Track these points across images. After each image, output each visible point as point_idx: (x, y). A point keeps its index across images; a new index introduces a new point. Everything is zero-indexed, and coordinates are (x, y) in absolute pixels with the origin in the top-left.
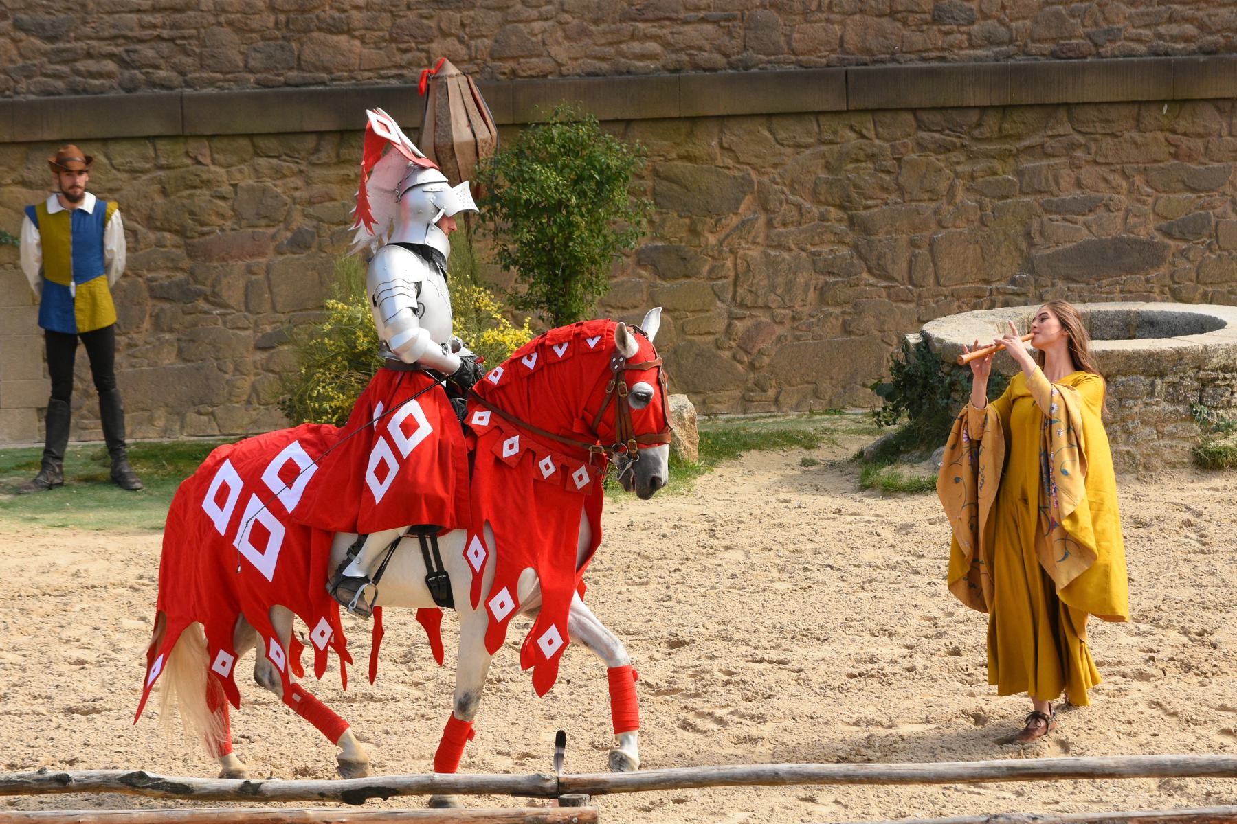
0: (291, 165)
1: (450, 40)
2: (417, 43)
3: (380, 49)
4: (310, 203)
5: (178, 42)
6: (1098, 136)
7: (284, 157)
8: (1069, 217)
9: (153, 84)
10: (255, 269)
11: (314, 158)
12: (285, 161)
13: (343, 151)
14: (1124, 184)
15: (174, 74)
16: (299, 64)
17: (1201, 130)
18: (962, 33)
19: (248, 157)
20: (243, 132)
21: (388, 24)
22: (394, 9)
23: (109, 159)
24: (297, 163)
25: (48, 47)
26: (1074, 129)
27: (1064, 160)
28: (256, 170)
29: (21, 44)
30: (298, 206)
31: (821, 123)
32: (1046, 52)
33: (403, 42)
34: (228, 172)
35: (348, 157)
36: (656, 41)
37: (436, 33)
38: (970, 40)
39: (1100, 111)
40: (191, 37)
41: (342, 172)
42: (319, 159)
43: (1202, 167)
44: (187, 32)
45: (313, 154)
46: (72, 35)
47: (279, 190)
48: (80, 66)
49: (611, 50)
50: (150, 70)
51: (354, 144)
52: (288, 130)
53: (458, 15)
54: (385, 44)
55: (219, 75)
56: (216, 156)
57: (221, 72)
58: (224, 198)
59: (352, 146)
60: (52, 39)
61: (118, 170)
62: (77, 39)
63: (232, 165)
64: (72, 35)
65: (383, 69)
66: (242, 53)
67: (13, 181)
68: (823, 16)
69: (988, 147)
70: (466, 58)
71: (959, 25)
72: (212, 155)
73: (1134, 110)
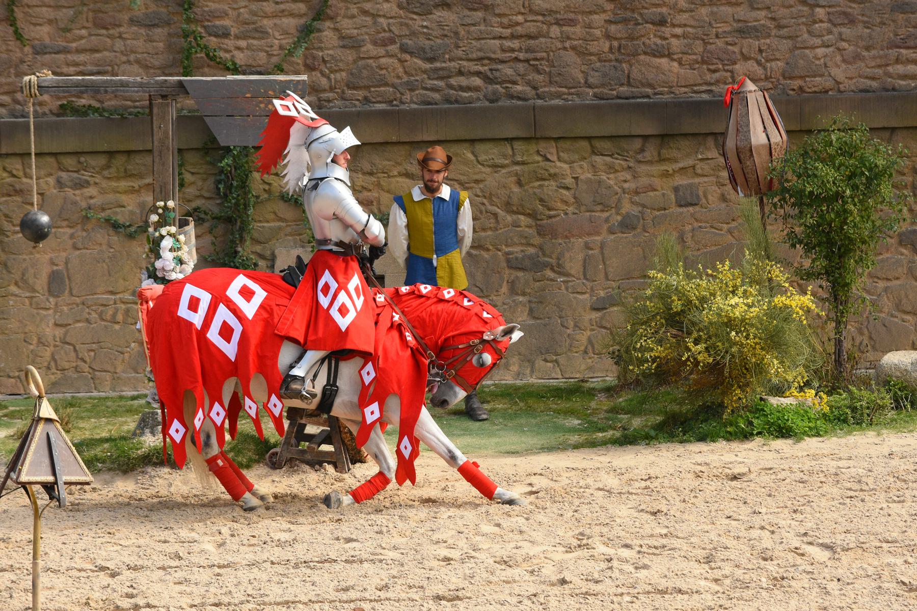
0: (621, 162)
1: (750, 62)
2: (724, 65)
3: (694, 69)
4: (637, 193)
5: (532, 62)
7: (616, 156)
9: (512, 97)
10: (591, 245)
11: (640, 157)
12: (617, 159)
13: (664, 151)
15: (528, 89)
16: (629, 82)
19: (586, 155)
23: (476, 156)
24: (626, 160)
25: (428, 66)
28: (593, 166)
40: (542, 59)
44: (539, 55)
45: (639, 153)
46: (447, 56)
47: (612, 182)
48: (453, 81)
50: (510, 85)
55: (564, 90)
56: (562, 154)
57: (566, 87)
58: (568, 188)
59: (671, 147)
60: (432, 60)
61: (483, 165)
62: (451, 60)
63: (573, 162)
64: (447, 56)
66: (583, 72)
67: (399, 173)
70: (763, 77)
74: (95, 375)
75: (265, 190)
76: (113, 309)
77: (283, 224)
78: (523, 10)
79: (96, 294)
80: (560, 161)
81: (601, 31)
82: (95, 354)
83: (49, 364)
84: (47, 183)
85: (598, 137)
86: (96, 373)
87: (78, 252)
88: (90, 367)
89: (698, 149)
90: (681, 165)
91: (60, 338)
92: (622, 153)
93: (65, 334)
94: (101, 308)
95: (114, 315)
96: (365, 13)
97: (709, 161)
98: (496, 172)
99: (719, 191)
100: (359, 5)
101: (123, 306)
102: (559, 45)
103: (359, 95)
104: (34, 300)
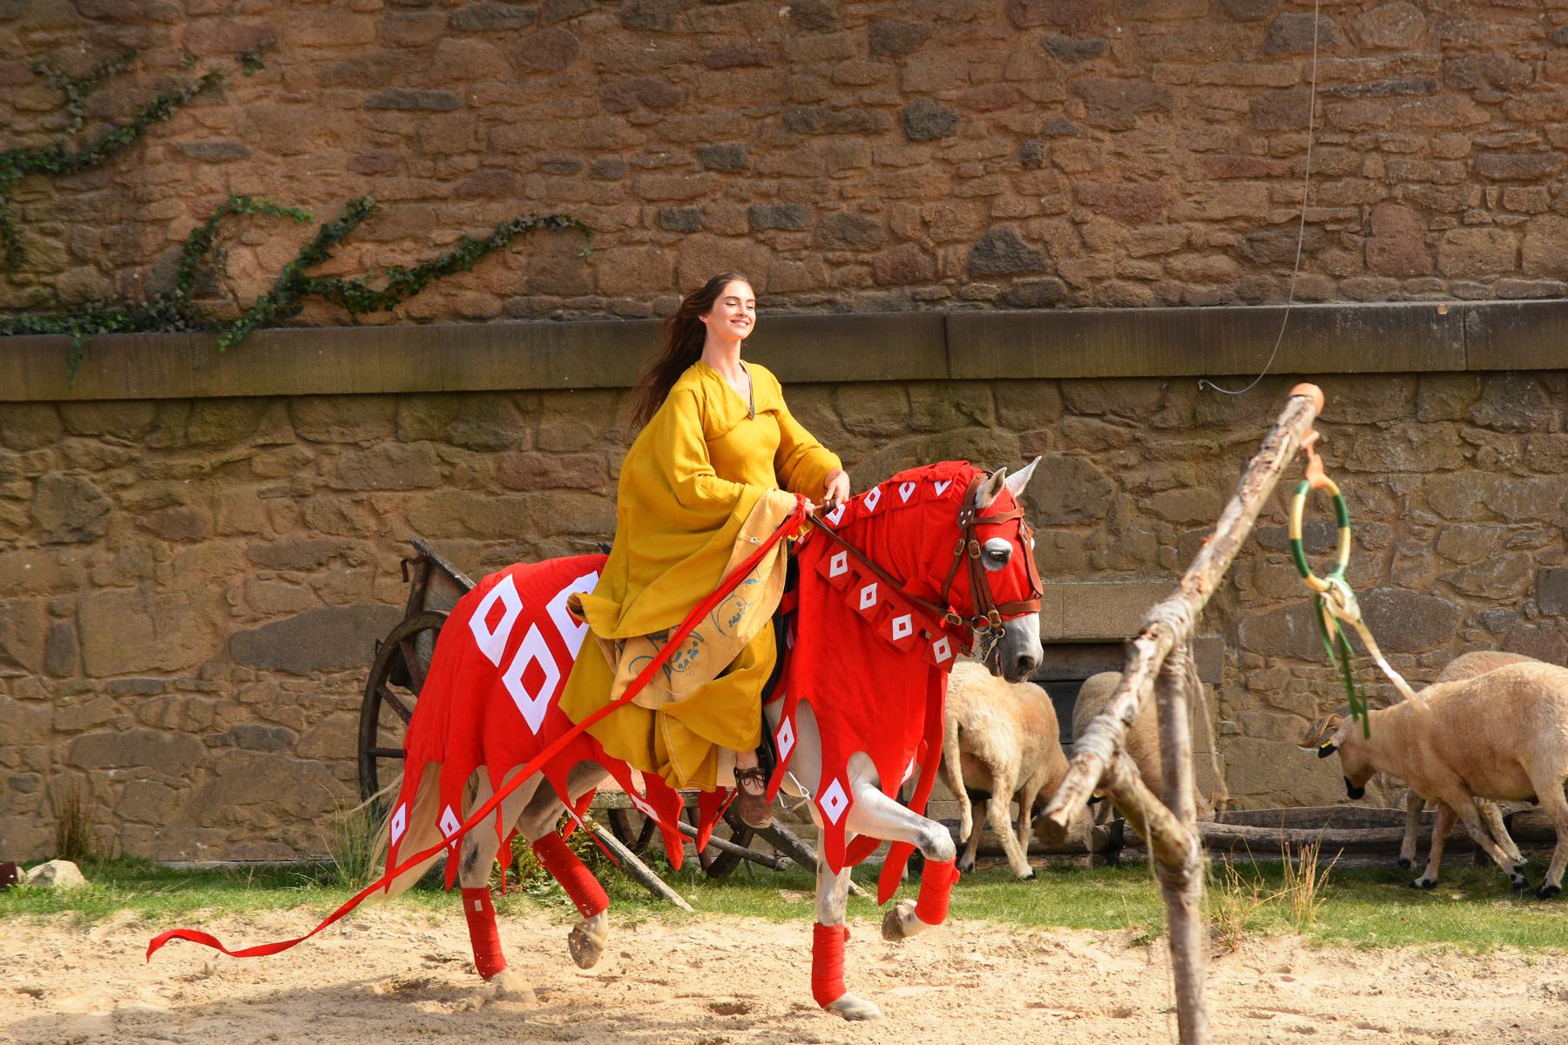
0: (1121, 430)
4: (143, 508)
5: (1330, 227)
6: (335, 449)
7: (109, 437)
8: (287, 574)
10: (58, 610)
11: (1156, 420)
12: (109, 443)
14: (372, 523)
15: (488, 297)
17: (492, 441)
18: (863, 263)
19: (54, 436)
20: (378, 390)
21: (814, 220)
22: (818, 198)
24: (1130, 426)
25: (1125, 232)
26: (298, 436)
27: (282, 483)
28: (65, 456)
29: (1085, 228)
30: (1127, 495)
31: (912, 399)
32: (992, 296)
33: (833, 250)
34: (24, 458)
35: (201, 439)
36: (1226, 253)
37: (65, 258)
38: (874, 275)
39: (335, 406)
41: (1199, 442)
42: (1164, 420)
43: (492, 499)
44: (1342, 213)
45: (1157, 412)
46: (1165, 212)
47: (99, 489)
48: (1176, 263)
49: (1153, 267)
51: (209, 418)
52: (83, 398)
53: (917, 208)
54: (805, 253)
55: (556, 299)
56: (1004, 411)
57: (558, 294)
58: (16, 499)
59: (395, 423)
60: (1134, 220)
61: (851, 432)
62: (1171, 221)
63: (29, 449)
64: (1165, 212)
65: (803, 292)
68: (646, 235)
69: (1175, 443)
71: (37, 273)
72: (997, 411)
73: (389, 409)
74: (123, 829)
75: (443, 476)
76: (161, 703)
77: (476, 543)
78: (473, 145)
79: (130, 673)
80: (1000, 425)
81: (1466, 164)
82: (126, 789)
83: (40, 806)
84: (41, 457)
85: (1077, 379)
86: (127, 825)
87: (96, 592)
88: (114, 813)
89: (258, 425)
90: (1235, 437)
91: (63, 757)
92: (116, 432)
93: (73, 749)
94: (141, 701)
95: (161, 716)
96: (1004, 129)
97: (277, 450)
98: (876, 447)
99: (296, 508)
100: (165, 140)
101: (179, 697)
102: (1382, 192)
103: (990, 290)
104: (17, 683)
